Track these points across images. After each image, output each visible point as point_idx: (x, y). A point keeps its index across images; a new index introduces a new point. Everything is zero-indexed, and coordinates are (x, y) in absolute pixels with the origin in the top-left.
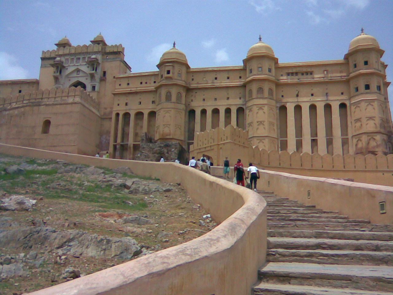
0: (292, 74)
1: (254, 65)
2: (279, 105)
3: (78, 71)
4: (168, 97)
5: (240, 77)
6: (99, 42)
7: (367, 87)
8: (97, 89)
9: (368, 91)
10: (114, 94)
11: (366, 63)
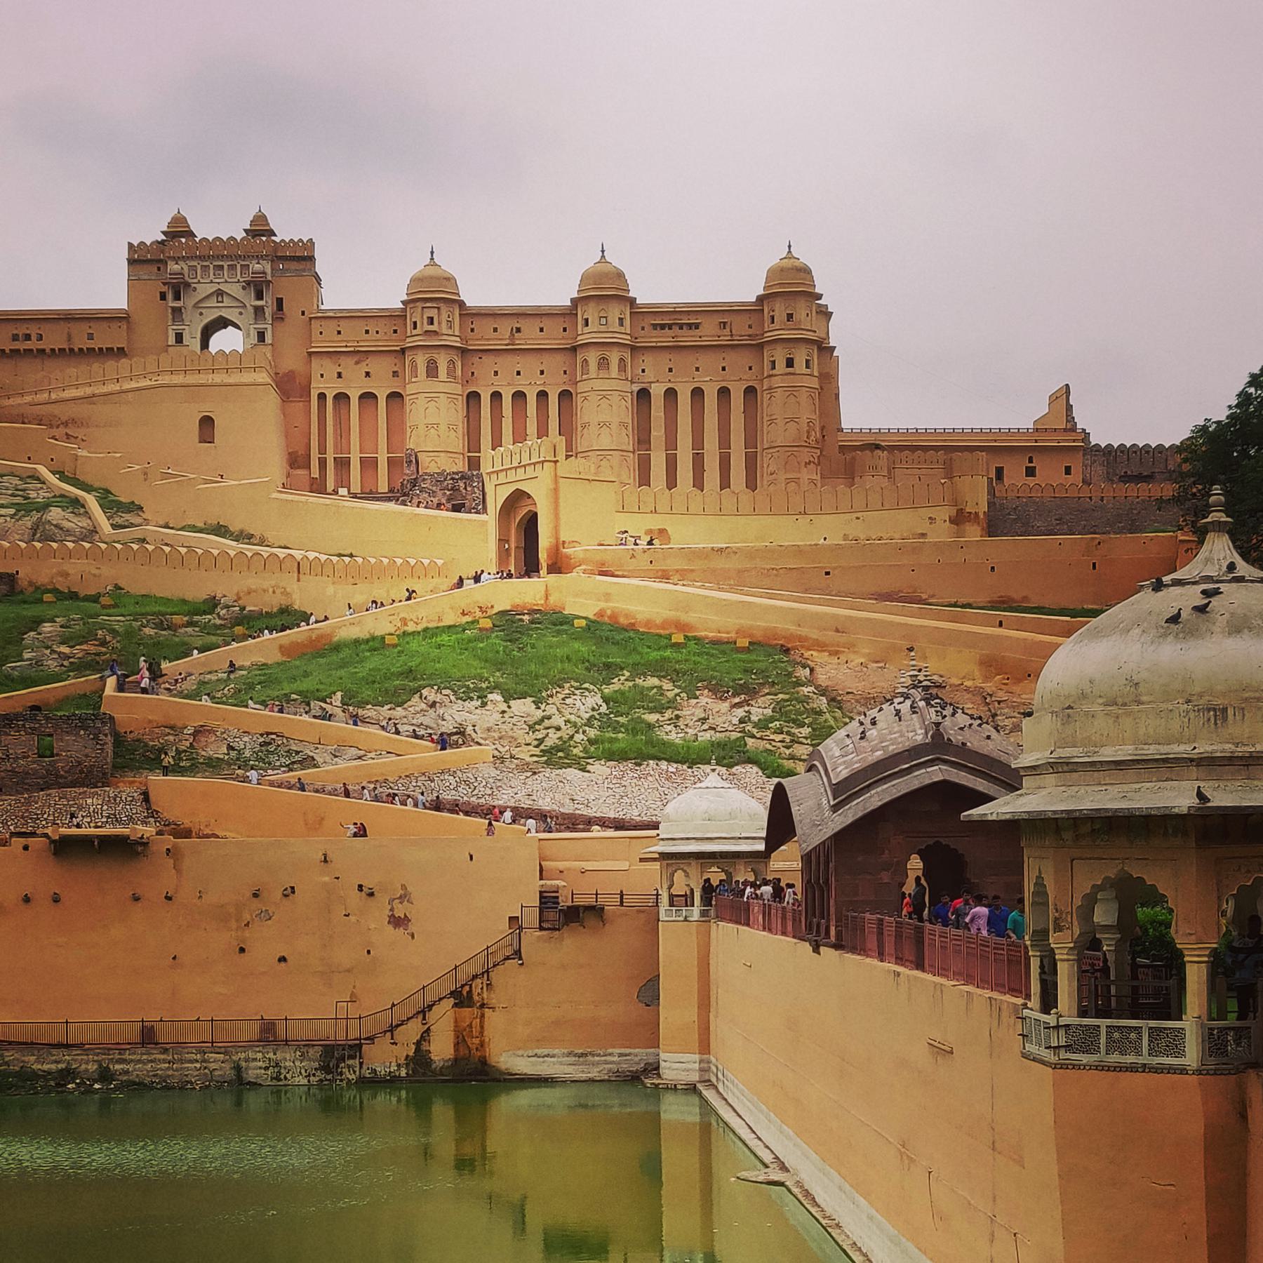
0: (663, 327)
1: (591, 312)
2: (636, 388)
3: (220, 293)
4: (432, 371)
5: (565, 330)
6: (260, 229)
7: (790, 363)
8: (268, 339)
9: (790, 370)
10: (310, 354)
11: (790, 316)
